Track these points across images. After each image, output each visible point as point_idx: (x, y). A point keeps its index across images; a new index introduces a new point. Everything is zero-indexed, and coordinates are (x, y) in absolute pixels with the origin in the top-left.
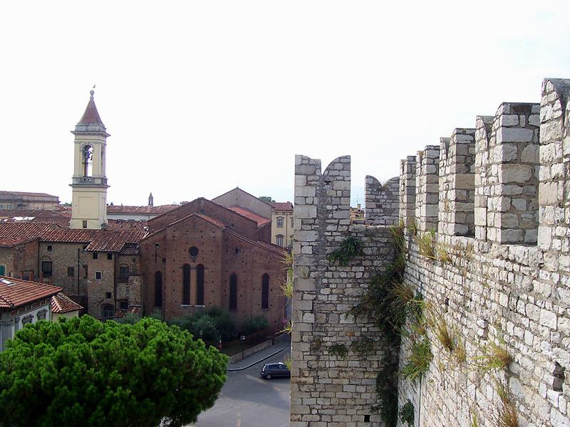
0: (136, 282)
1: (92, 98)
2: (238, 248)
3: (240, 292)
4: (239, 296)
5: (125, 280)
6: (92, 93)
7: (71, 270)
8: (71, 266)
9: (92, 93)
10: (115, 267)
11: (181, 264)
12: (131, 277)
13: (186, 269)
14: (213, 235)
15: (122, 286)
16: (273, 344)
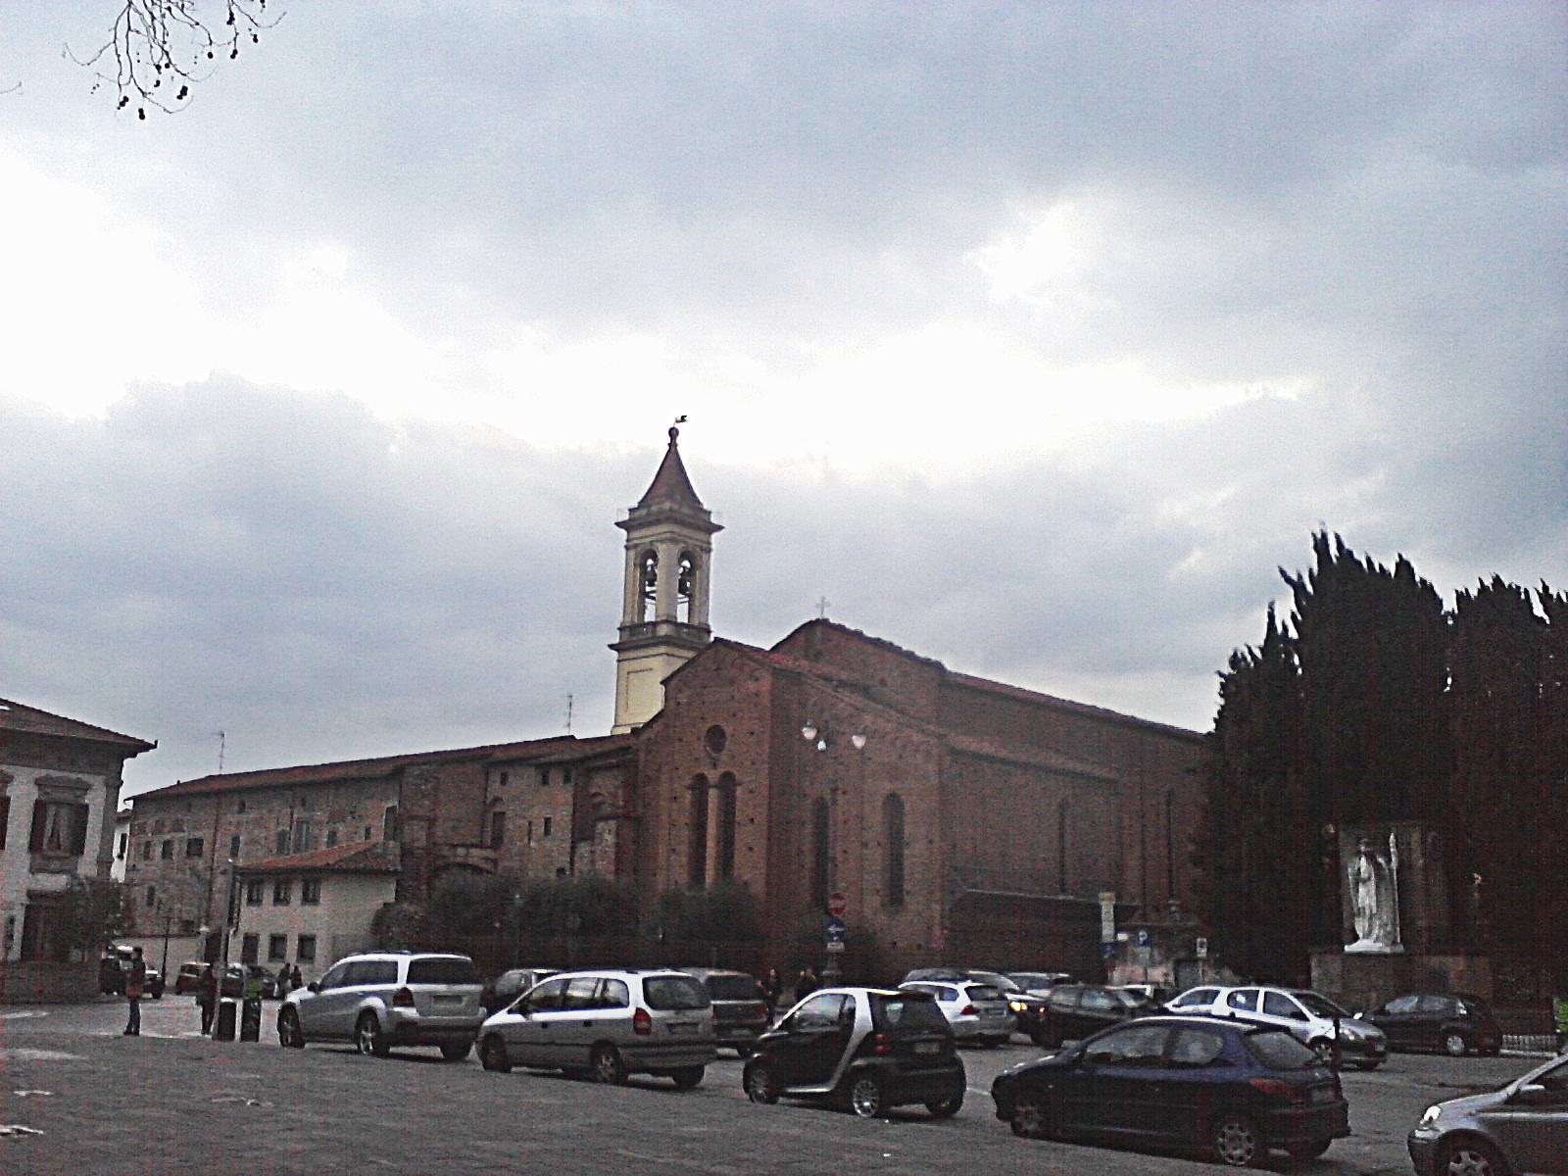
0: (607, 835)
1: (673, 445)
6: (673, 433)
9: (673, 433)
12: (600, 825)
13: (700, 784)
14: (752, 686)
15: (584, 848)
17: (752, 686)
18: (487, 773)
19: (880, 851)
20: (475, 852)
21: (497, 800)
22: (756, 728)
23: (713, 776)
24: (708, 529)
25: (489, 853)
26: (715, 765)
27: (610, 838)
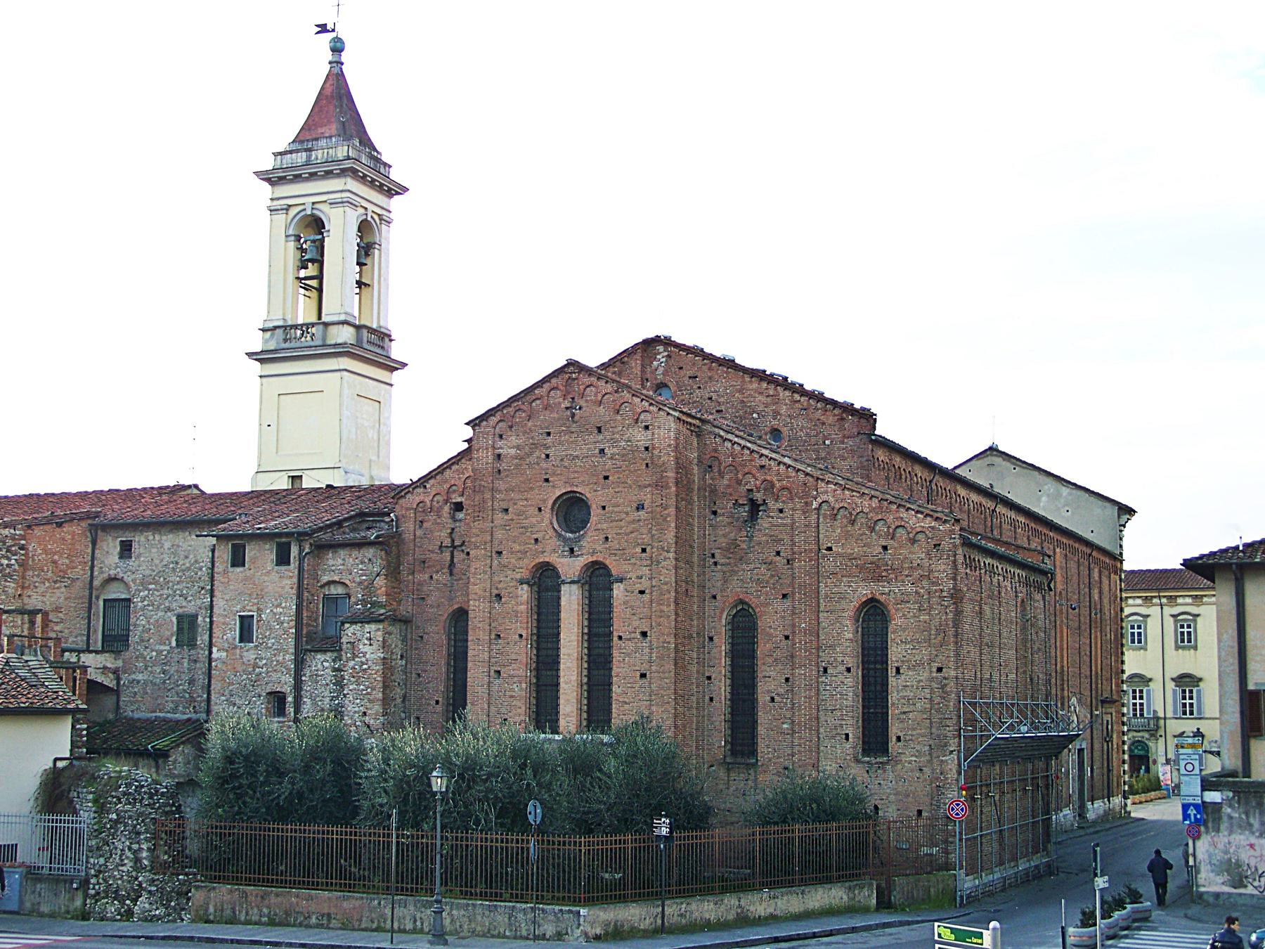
2: (759, 496)
3: (769, 682)
4: (762, 698)
5: (331, 644)
7: (187, 627)
8: (190, 608)
10: (299, 596)
11: (529, 563)
12: (350, 630)
14: (641, 438)
15: (321, 663)
16: (884, 904)
17: (641, 438)
18: (94, 543)
19: (849, 681)
20: (87, 659)
21: (112, 579)
22: (647, 497)
23: (570, 567)
24: (390, 189)
25: (107, 660)
26: (572, 550)
27: (371, 653)
